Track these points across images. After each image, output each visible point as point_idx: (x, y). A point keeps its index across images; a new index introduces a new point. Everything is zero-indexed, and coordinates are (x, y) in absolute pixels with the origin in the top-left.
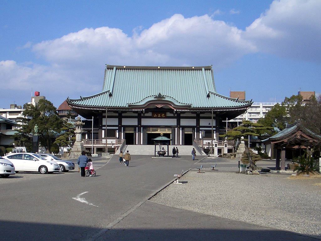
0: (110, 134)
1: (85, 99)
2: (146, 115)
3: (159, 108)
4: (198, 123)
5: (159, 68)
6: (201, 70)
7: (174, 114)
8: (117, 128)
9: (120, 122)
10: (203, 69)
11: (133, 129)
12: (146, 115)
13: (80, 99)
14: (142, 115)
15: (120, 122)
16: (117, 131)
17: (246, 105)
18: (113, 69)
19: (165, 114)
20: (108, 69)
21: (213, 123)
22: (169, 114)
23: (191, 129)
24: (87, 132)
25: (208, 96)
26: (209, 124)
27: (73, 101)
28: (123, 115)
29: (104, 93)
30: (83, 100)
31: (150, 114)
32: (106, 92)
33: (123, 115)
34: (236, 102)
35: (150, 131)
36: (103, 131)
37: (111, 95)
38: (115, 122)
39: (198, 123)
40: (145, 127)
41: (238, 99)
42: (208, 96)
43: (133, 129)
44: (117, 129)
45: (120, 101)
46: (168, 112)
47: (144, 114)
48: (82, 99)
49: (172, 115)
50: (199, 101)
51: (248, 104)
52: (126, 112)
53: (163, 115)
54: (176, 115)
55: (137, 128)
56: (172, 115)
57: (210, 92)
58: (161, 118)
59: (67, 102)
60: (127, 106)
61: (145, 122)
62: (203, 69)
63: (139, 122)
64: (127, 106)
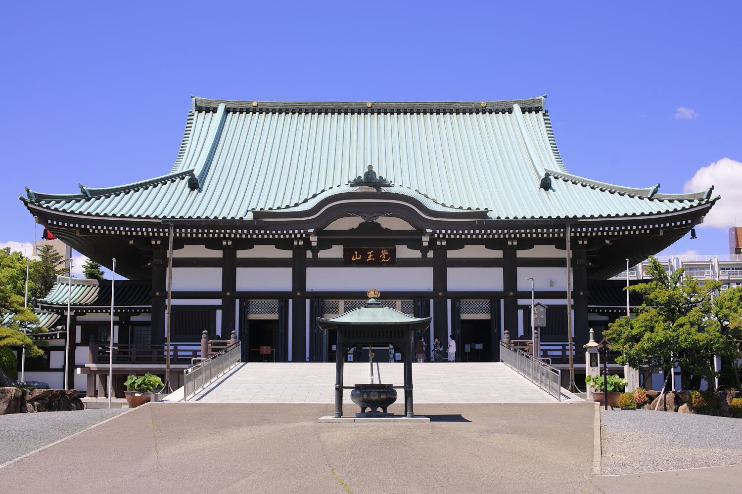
0: (193, 322)
1: (97, 194)
2: (323, 254)
3: (370, 224)
4: (510, 279)
6: (510, 111)
7: (424, 251)
8: (218, 302)
9: (229, 279)
10: (517, 108)
11: (275, 303)
12: (323, 254)
13: (80, 194)
14: (309, 255)
15: (229, 279)
16: (219, 313)
17: (692, 207)
18: (215, 111)
19: (392, 253)
20: (200, 110)
21: (561, 279)
22: (403, 252)
23: (486, 302)
25: (546, 185)
26: (552, 283)
27: (49, 199)
28: (241, 254)
29: (172, 179)
30: (89, 200)
31: (336, 252)
32: (181, 176)
33: (241, 254)
34: (651, 199)
36: (167, 312)
37: (194, 185)
38: (211, 279)
39: (510, 279)
40: (323, 301)
41: (655, 192)
42: (546, 185)
43: (275, 303)
44: (218, 307)
45: (228, 199)
46: (401, 242)
47: (315, 251)
48: (87, 196)
49: (417, 254)
50: (514, 198)
51: (699, 204)
52: (248, 244)
53: (385, 253)
54: (430, 254)
55: (291, 301)
56: (417, 254)
57: (547, 175)
58: (377, 263)
59: (26, 204)
60: (250, 216)
61: (318, 280)
62: (517, 108)
63: (299, 279)
64: (250, 216)
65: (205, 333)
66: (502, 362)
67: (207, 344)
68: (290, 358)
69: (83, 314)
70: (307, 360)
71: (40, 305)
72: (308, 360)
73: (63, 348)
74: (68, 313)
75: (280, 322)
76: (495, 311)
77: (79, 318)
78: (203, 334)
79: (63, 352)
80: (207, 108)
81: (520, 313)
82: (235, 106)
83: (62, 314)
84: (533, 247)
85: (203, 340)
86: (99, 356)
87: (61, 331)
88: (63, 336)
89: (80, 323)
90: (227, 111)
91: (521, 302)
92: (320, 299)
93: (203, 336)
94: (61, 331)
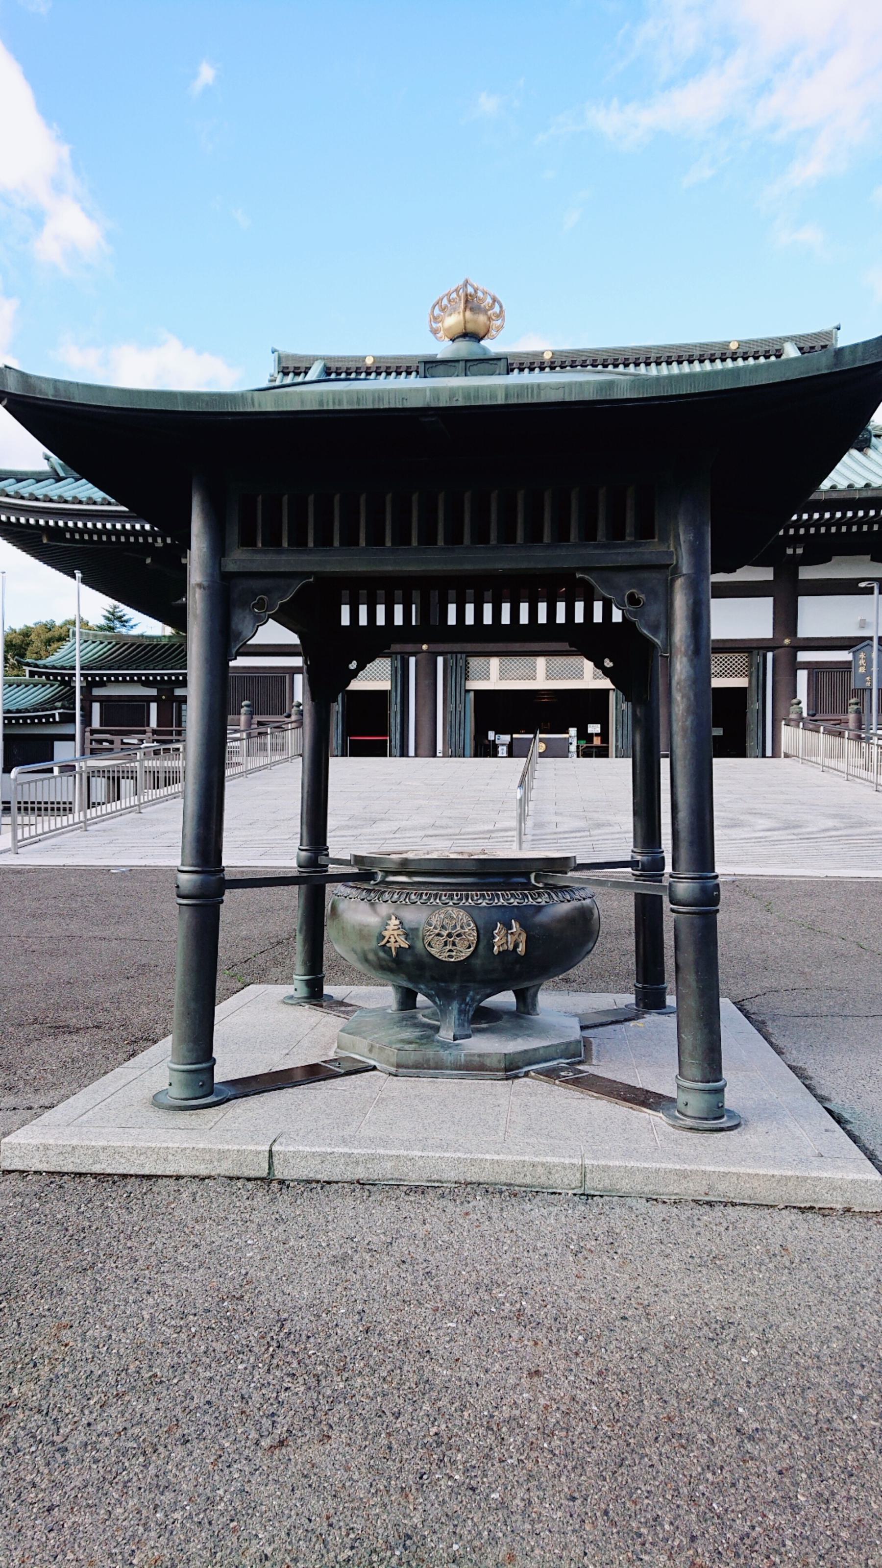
5: (547, 356)
24: (153, 692)
26: (863, 624)
35: (487, 677)
44: (298, 670)
55: (412, 660)
65: (247, 706)
66: (787, 756)
67: (249, 724)
68: (412, 752)
69: (102, 684)
70: (438, 755)
71: (27, 669)
72: (441, 755)
73: (72, 738)
74: (78, 683)
75: (393, 694)
76: (758, 674)
77: (97, 692)
78: (242, 707)
79: (73, 743)
80: (295, 368)
81: (802, 676)
82: (339, 365)
83: (67, 682)
84: (830, 560)
85: (243, 718)
86: (92, 747)
87: (61, 711)
88: (71, 719)
89: (99, 699)
90: (327, 371)
91: (803, 656)
92: (459, 656)
93: (243, 710)
94: (61, 711)
